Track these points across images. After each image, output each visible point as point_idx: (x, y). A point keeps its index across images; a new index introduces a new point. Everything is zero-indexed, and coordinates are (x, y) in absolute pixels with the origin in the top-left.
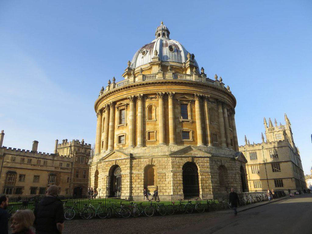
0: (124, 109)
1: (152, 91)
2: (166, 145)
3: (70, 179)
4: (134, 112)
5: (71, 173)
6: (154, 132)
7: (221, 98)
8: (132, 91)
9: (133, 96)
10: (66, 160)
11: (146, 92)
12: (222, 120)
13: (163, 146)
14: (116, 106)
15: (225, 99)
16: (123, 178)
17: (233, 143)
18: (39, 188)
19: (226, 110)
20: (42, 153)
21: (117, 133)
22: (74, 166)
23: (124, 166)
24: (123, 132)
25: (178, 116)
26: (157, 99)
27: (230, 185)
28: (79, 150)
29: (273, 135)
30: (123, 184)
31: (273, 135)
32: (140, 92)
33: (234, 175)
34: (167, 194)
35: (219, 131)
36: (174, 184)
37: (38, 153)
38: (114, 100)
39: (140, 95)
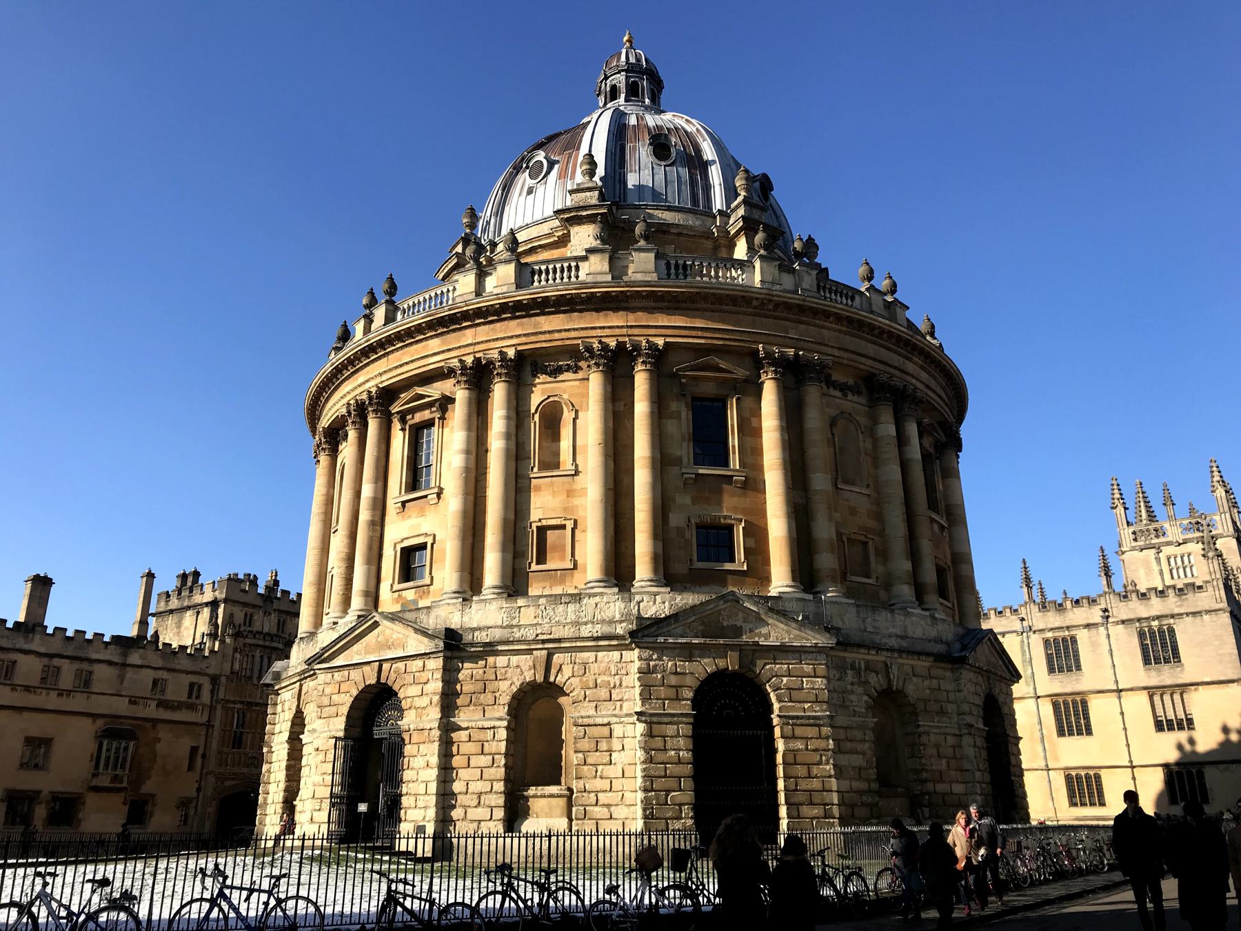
1: (557, 336)
2: (616, 590)
3: (204, 756)
4: (474, 434)
5: (209, 725)
6: (563, 527)
7: (892, 370)
8: (468, 336)
9: (469, 360)
10: (184, 663)
11: (533, 339)
12: (893, 472)
13: (601, 594)
14: (395, 408)
15: (909, 378)
16: (408, 749)
17: (951, 585)
18: (45, 793)
19: (912, 429)
20: (70, 633)
21: (398, 531)
22: (221, 696)
23: (414, 690)
25: (678, 453)
26: (580, 375)
27: (930, 786)
28: (249, 620)
29: (1158, 560)
30: (407, 775)
31: (1158, 560)
32: (503, 339)
33: (950, 740)
34: (615, 826)
35: (871, 523)
36: (647, 777)
37: (50, 631)
39: (501, 353)
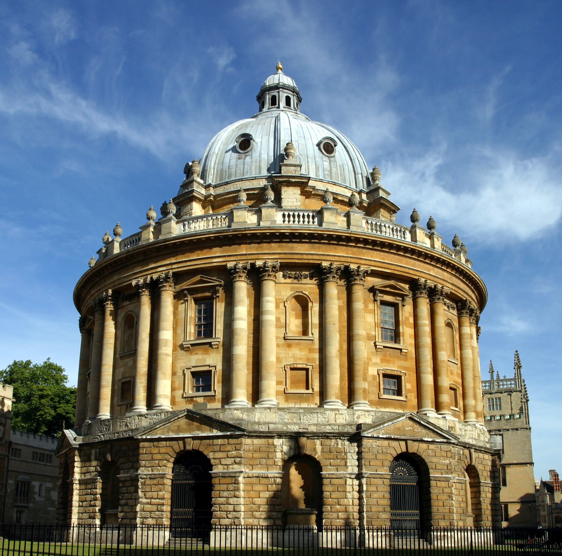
6: (307, 370)
13: (338, 410)
16: (217, 487)
24: (207, 363)
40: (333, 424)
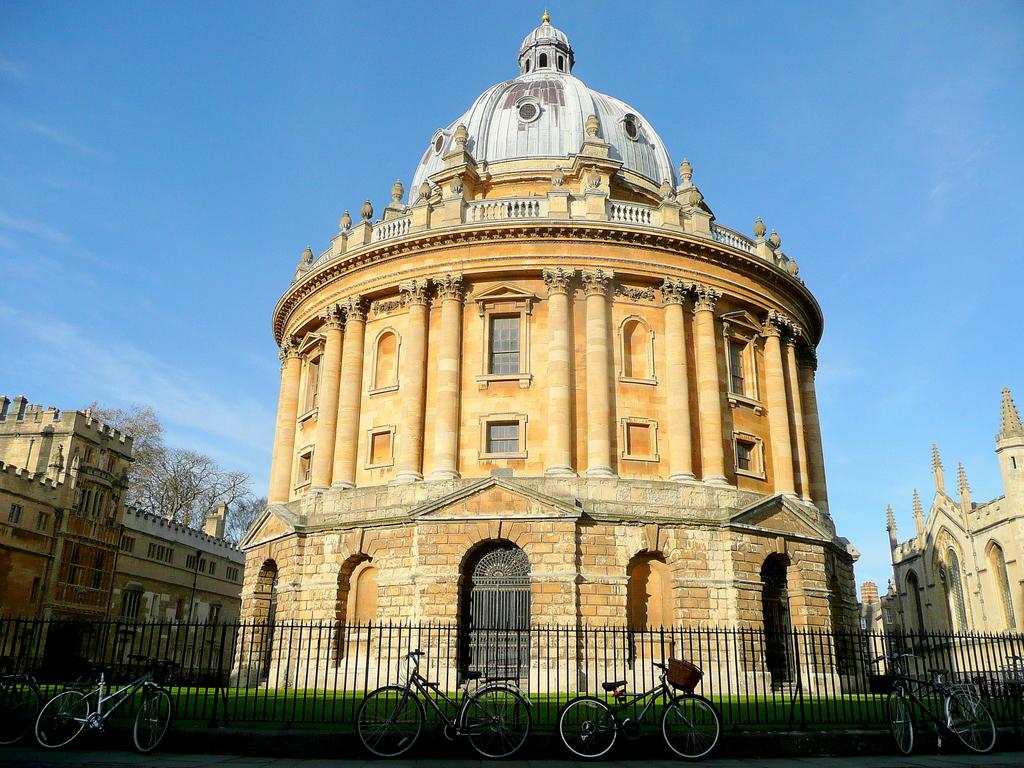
0: (517, 315)
1: (645, 268)
13: (693, 487)
22: (64, 529)
23: (542, 548)
38: (470, 269)
40: (690, 507)
